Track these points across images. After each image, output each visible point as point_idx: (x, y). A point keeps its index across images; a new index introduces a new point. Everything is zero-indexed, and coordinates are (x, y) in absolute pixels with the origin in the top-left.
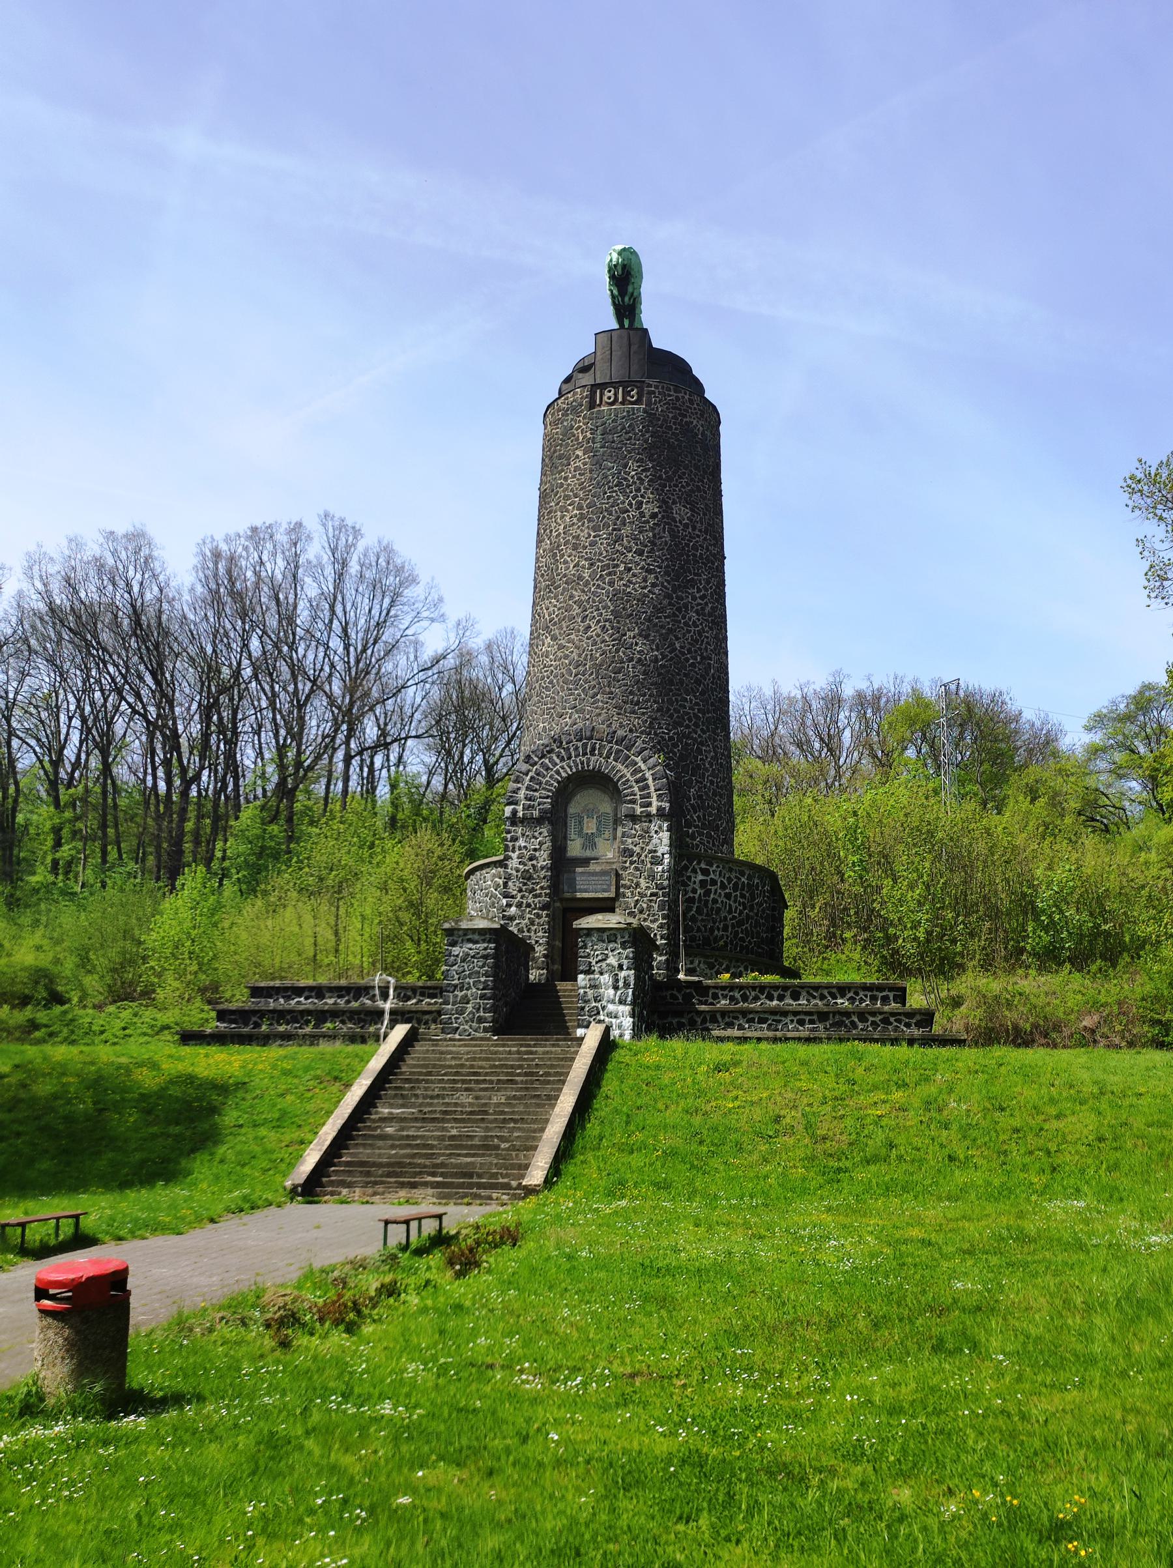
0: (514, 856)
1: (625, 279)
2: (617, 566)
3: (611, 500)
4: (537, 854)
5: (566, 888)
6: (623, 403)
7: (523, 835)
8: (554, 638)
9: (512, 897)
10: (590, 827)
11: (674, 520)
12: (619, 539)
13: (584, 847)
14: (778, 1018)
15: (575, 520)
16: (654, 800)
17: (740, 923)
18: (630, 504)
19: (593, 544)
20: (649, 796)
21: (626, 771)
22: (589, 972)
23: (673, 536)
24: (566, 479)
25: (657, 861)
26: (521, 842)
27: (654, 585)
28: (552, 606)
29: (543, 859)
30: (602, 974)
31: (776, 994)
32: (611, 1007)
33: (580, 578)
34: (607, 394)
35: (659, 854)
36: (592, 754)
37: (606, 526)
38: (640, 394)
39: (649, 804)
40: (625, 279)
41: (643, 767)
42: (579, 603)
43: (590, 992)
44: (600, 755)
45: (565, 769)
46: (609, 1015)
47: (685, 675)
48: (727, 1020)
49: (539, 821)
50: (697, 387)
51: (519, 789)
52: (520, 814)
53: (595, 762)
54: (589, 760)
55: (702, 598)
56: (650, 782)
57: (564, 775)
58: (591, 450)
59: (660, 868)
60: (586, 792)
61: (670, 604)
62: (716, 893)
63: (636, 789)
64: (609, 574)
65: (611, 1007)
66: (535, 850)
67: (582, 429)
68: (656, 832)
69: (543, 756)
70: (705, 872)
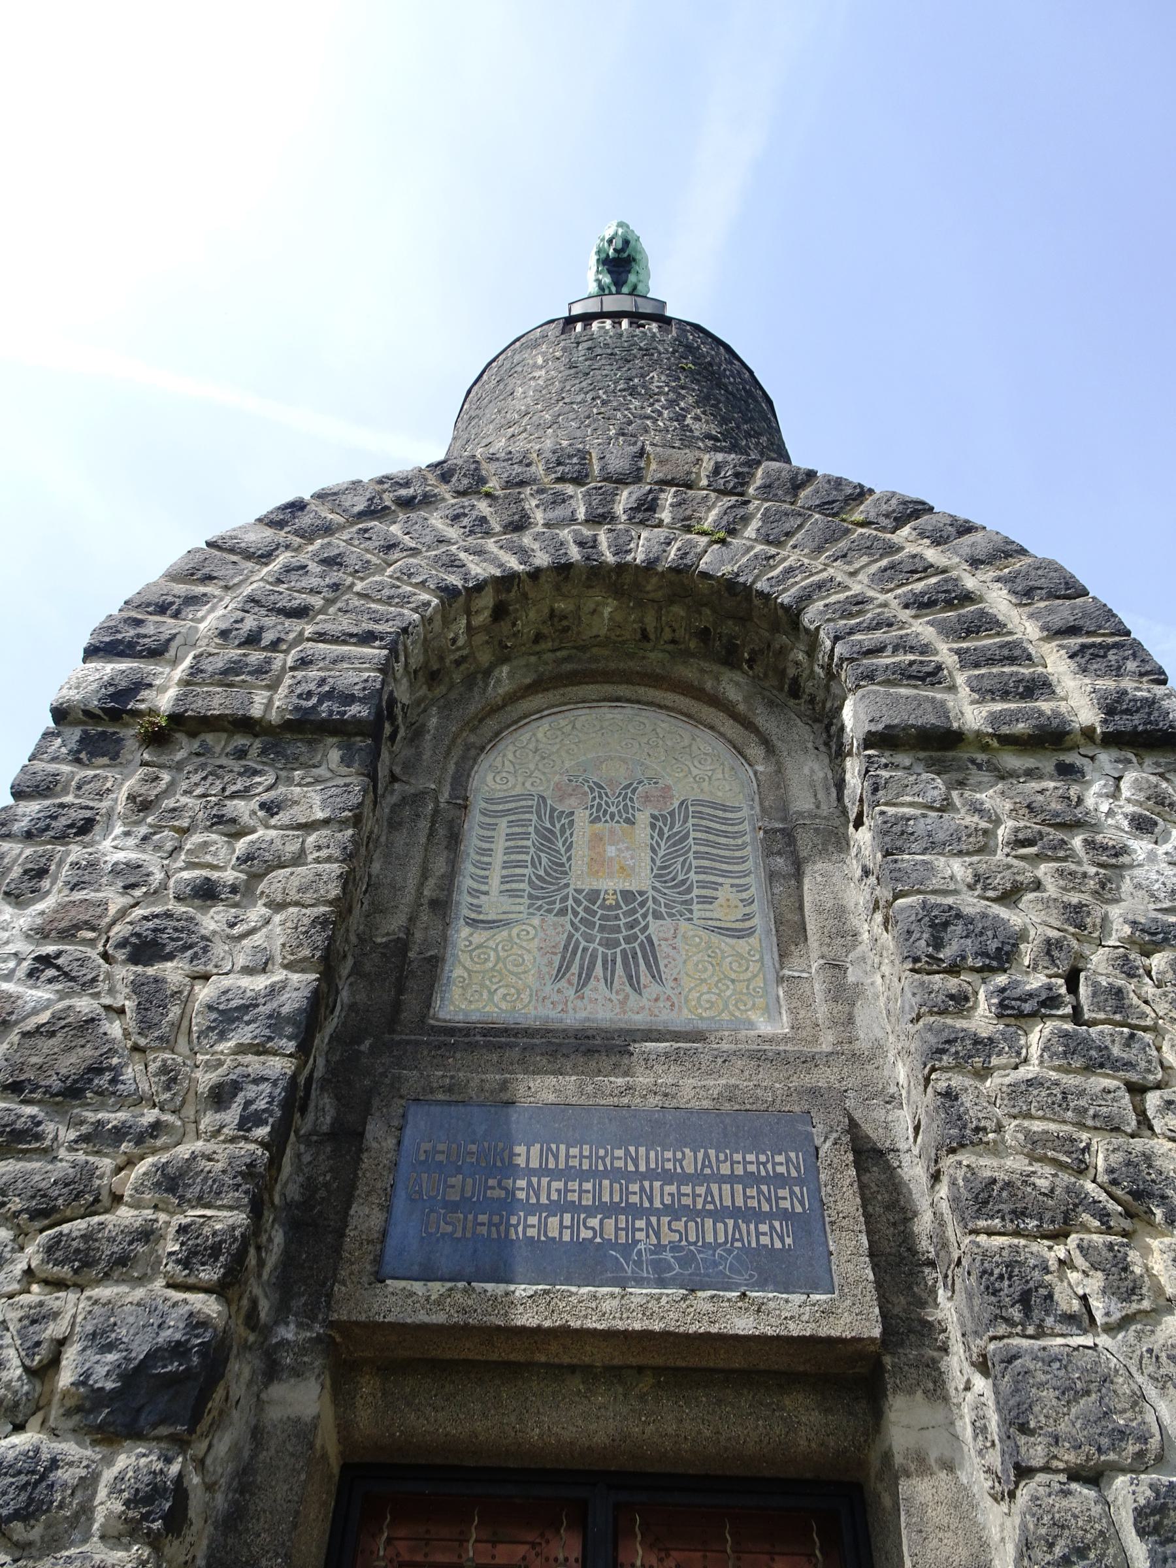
4: (212, 920)
5: (407, 1231)
13: (571, 965)
26: (114, 847)
29: (258, 957)
49: (299, 734)
60: (584, 717)
68: (1142, 825)
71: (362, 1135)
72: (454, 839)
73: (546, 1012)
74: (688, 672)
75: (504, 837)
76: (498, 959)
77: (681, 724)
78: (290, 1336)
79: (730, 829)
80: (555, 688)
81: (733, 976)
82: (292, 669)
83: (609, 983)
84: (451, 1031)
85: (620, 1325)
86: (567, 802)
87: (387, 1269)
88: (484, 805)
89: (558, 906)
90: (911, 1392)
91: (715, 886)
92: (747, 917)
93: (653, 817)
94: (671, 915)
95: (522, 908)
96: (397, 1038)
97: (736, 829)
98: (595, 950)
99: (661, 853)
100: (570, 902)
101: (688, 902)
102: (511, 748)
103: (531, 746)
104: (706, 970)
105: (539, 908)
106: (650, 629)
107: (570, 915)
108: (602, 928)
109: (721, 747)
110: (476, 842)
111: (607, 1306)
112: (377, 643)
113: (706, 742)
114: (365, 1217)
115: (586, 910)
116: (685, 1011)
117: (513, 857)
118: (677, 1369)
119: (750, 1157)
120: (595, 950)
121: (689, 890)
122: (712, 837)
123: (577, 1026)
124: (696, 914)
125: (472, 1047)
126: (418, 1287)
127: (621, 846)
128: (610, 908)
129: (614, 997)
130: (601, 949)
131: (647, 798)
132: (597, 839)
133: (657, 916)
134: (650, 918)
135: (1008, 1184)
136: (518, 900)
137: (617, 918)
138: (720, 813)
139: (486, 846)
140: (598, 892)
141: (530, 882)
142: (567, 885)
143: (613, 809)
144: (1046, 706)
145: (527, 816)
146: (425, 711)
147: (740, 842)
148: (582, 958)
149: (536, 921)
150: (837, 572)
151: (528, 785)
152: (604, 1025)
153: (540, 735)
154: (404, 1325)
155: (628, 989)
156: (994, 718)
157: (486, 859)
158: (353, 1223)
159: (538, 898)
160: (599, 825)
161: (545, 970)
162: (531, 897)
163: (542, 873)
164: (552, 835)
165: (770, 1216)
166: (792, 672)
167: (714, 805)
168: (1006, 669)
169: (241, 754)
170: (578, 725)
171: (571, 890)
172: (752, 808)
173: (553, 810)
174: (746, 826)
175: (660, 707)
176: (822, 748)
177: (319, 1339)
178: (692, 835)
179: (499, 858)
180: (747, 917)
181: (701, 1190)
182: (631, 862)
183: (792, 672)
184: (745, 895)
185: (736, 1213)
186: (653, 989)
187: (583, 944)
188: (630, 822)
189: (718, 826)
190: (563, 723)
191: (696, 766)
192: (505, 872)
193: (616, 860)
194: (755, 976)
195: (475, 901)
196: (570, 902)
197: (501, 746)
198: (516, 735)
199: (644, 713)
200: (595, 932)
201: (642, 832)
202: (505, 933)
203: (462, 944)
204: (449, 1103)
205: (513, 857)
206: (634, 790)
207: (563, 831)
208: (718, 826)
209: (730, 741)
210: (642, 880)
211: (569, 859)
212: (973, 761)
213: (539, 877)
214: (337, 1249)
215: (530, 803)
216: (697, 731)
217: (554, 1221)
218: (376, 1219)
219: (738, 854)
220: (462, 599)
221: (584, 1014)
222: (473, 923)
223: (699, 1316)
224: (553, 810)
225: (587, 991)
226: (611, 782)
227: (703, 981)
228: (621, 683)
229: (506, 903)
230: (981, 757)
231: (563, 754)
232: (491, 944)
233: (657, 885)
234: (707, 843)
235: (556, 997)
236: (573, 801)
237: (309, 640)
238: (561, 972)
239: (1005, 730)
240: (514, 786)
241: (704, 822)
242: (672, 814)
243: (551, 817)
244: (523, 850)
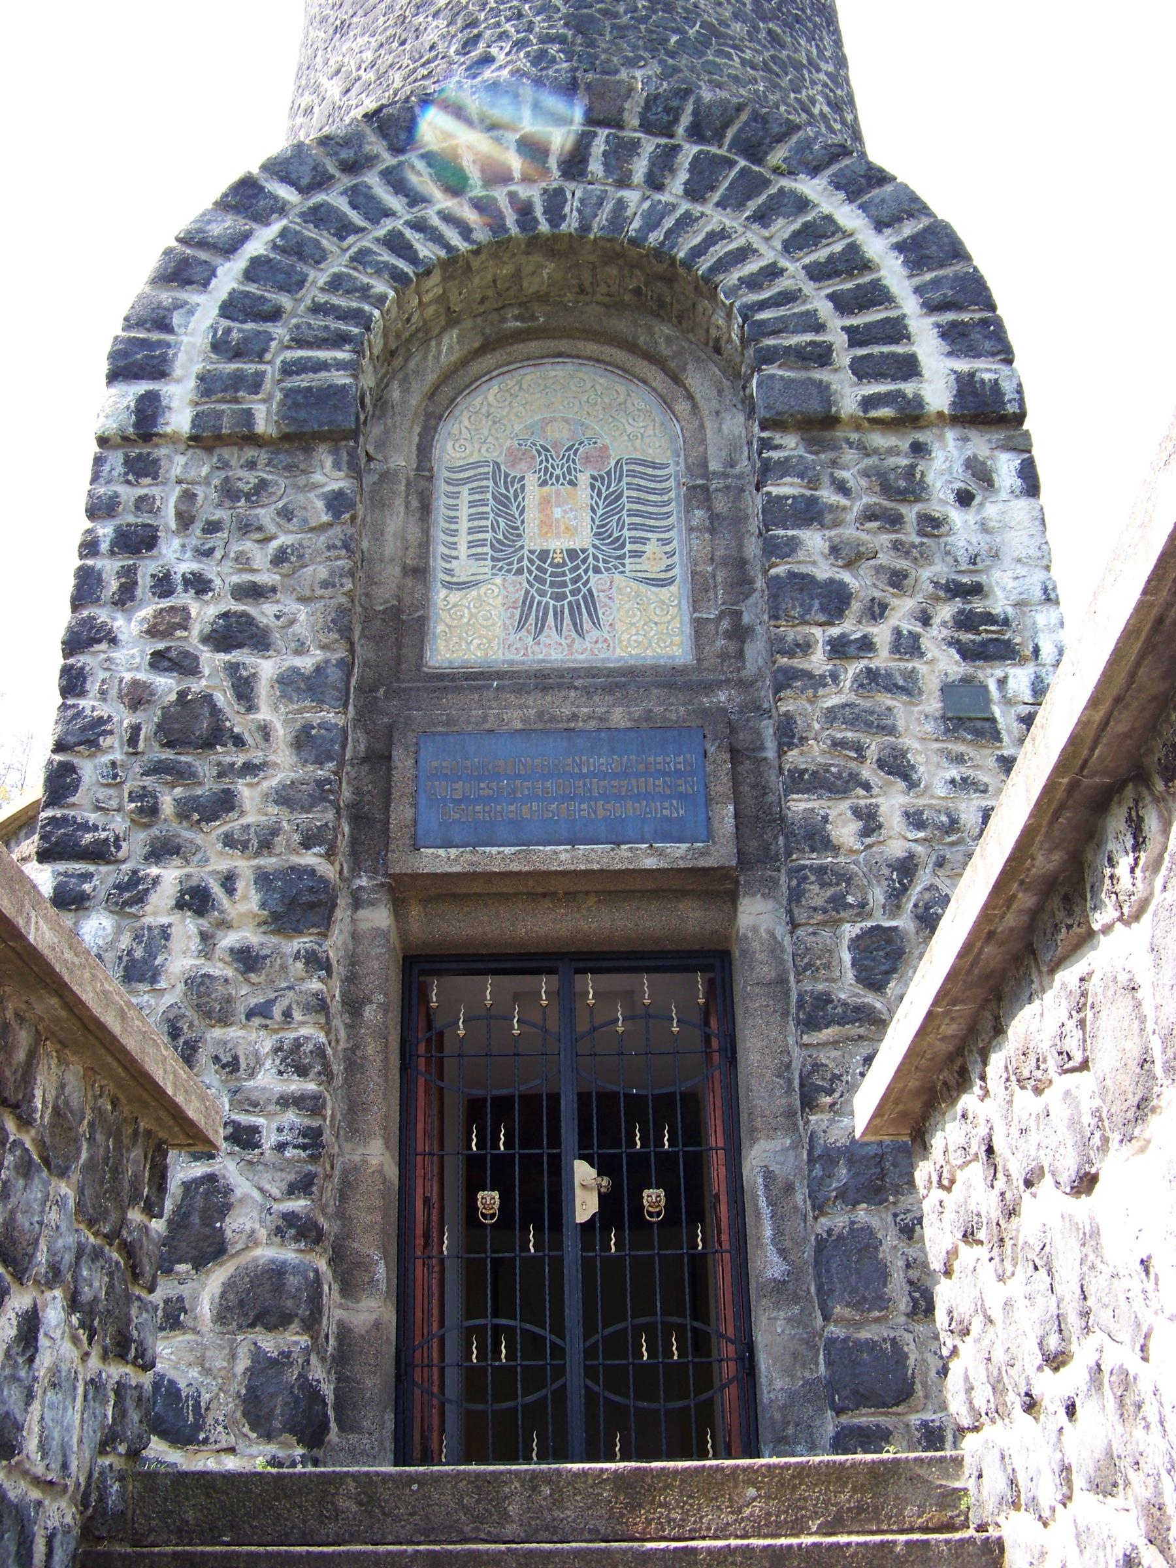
7: (185, 520)
9: (100, 853)
13: (530, 615)
20: (896, 331)
35: (999, 604)
39: (909, 367)
60: (530, 376)
69: (321, 181)
71: (389, 758)
72: (426, 508)
73: (511, 657)
74: (622, 325)
75: (466, 505)
76: (472, 615)
77: (617, 379)
78: (364, 884)
79: (659, 486)
80: (501, 347)
81: (657, 619)
82: (280, 381)
83: (559, 631)
84: (441, 677)
85: (573, 867)
86: (518, 467)
87: (420, 843)
88: (447, 474)
89: (515, 566)
90: (754, 895)
91: (643, 541)
92: (669, 568)
93: (593, 477)
94: (607, 569)
95: (486, 570)
96: (403, 685)
97: (662, 485)
98: (547, 603)
99: (600, 512)
100: (526, 562)
101: (622, 557)
102: (466, 414)
103: (484, 411)
104: (634, 615)
105: (501, 569)
106: (587, 284)
107: (526, 574)
108: (552, 584)
109: (652, 399)
110: (443, 510)
111: (563, 857)
112: (347, 347)
113: (640, 399)
114: (401, 813)
115: (539, 568)
116: (618, 650)
117: (476, 523)
118: (610, 892)
119: (659, 759)
120: (547, 603)
121: (622, 546)
122: (642, 495)
123: (536, 667)
124: (628, 568)
125: (460, 689)
126: (441, 852)
127: (566, 507)
128: (558, 566)
129: (563, 642)
130: (552, 602)
131: (587, 459)
132: (545, 502)
133: (597, 570)
134: (590, 573)
135: (814, 773)
136: (483, 563)
137: (564, 574)
138: (649, 471)
139: (452, 514)
140: (547, 552)
141: (492, 546)
142: (522, 547)
143: (558, 472)
144: (908, 388)
145: (484, 483)
146: (387, 386)
147: (666, 498)
148: (537, 611)
149: (499, 581)
150: (753, 236)
151: (483, 451)
152: (556, 665)
153: (491, 398)
154: (436, 874)
155: (574, 634)
156: (868, 403)
157: (453, 527)
158: (393, 816)
159: (499, 560)
160: (546, 489)
161: (508, 622)
162: (493, 559)
163: (501, 537)
164: (507, 502)
165: (671, 797)
166: (714, 333)
167: (645, 463)
168: (886, 349)
169: (252, 465)
170: (525, 386)
171: (525, 552)
172: (678, 464)
173: (506, 475)
174: (672, 483)
175: (598, 361)
176: (739, 406)
177: (382, 885)
178: (626, 493)
179: (464, 525)
180: (669, 568)
181: (624, 783)
182: (574, 523)
183: (714, 333)
184: (668, 548)
185: (648, 796)
186: (595, 633)
187: (538, 598)
188: (572, 483)
189: (647, 484)
190: (511, 383)
192: (470, 538)
193: (562, 520)
194: (673, 618)
195: (448, 566)
196: (526, 562)
197: (457, 412)
198: (469, 399)
199: (584, 369)
200: (546, 587)
201: (583, 493)
202: (474, 593)
203: (441, 604)
204: (447, 733)
205: (476, 523)
206: (575, 453)
207: (516, 497)
208: (647, 484)
209: (661, 397)
210: (583, 539)
211: (523, 522)
212: (847, 440)
213: (499, 541)
214: (386, 831)
215: (486, 470)
216: (632, 387)
217: (525, 808)
218: (409, 813)
219: (664, 510)
220: (413, 286)
221: (540, 657)
222: (449, 585)
223: (622, 860)
224: (506, 475)
225: (542, 638)
226: (555, 444)
227: (633, 624)
228: (561, 338)
229: (474, 567)
230: (854, 436)
231: (512, 417)
232: (465, 602)
233: (597, 542)
234: (639, 501)
235: (518, 645)
236: (523, 466)
237: (288, 347)
238: (522, 623)
239: (873, 414)
240: (471, 455)
241: (636, 481)
242: (609, 473)
243: (505, 482)
244: (483, 516)
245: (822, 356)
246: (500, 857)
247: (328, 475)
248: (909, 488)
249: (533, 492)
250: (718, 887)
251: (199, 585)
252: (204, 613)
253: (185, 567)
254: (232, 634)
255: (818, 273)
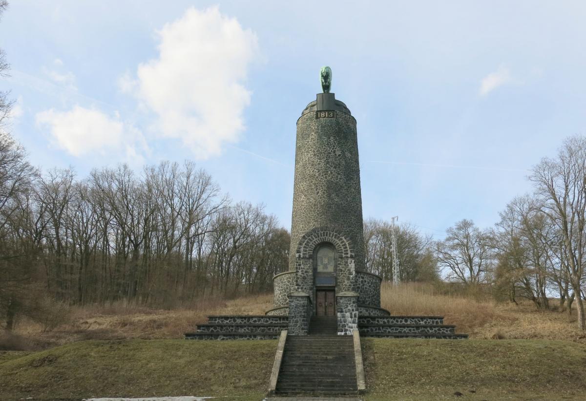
0: (300, 271)
1: (326, 77)
2: (327, 172)
3: (325, 150)
6: (328, 117)
7: (303, 264)
8: (305, 196)
9: (300, 286)
10: (326, 261)
11: (346, 157)
12: (328, 163)
13: (323, 268)
14: (402, 329)
15: (312, 156)
16: (349, 252)
17: (373, 296)
18: (332, 151)
19: (319, 164)
20: (347, 251)
21: (338, 242)
22: (342, 312)
23: (346, 163)
24: (308, 142)
25: (351, 274)
26: (302, 266)
27: (340, 179)
28: (304, 185)
30: (346, 312)
31: (399, 320)
32: (350, 325)
33: (315, 175)
34: (322, 114)
35: (351, 271)
36: (327, 235)
37: (324, 158)
38: (333, 115)
39: (347, 254)
40: (326, 77)
41: (345, 241)
42: (315, 184)
43: (342, 319)
44: (330, 236)
45: (316, 241)
46: (350, 327)
47: (351, 210)
48: (384, 329)
50: (348, 112)
51: (301, 247)
52: (302, 256)
53: (328, 239)
54: (325, 238)
55: (355, 184)
56: (348, 246)
57: (317, 243)
58: (317, 132)
59: (352, 276)
61: (346, 185)
62: (367, 286)
63: (342, 248)
64: (325, 174)
65: (350, 325)
66: (307, 269)
67: (314, 125)
69: (309, 236)
70: (363, 278)
164: (322, 260)
191: (331, 254)
245: (342, 252)
246: (322, 285)
247: (311, 261)
248: (347, 262)
249: (324, 259)
250: (334, 287)
251: (304, 268)
252: (304, 270)
253: (303, 267)
254: (306, 272)
255: (343, 246)
